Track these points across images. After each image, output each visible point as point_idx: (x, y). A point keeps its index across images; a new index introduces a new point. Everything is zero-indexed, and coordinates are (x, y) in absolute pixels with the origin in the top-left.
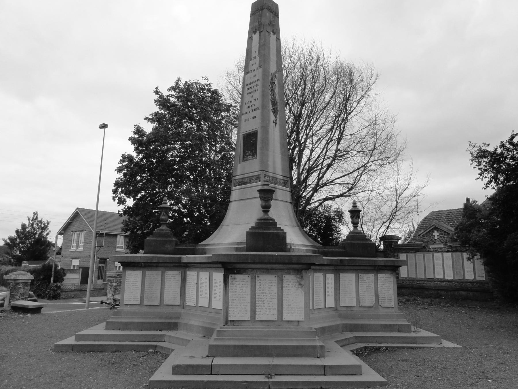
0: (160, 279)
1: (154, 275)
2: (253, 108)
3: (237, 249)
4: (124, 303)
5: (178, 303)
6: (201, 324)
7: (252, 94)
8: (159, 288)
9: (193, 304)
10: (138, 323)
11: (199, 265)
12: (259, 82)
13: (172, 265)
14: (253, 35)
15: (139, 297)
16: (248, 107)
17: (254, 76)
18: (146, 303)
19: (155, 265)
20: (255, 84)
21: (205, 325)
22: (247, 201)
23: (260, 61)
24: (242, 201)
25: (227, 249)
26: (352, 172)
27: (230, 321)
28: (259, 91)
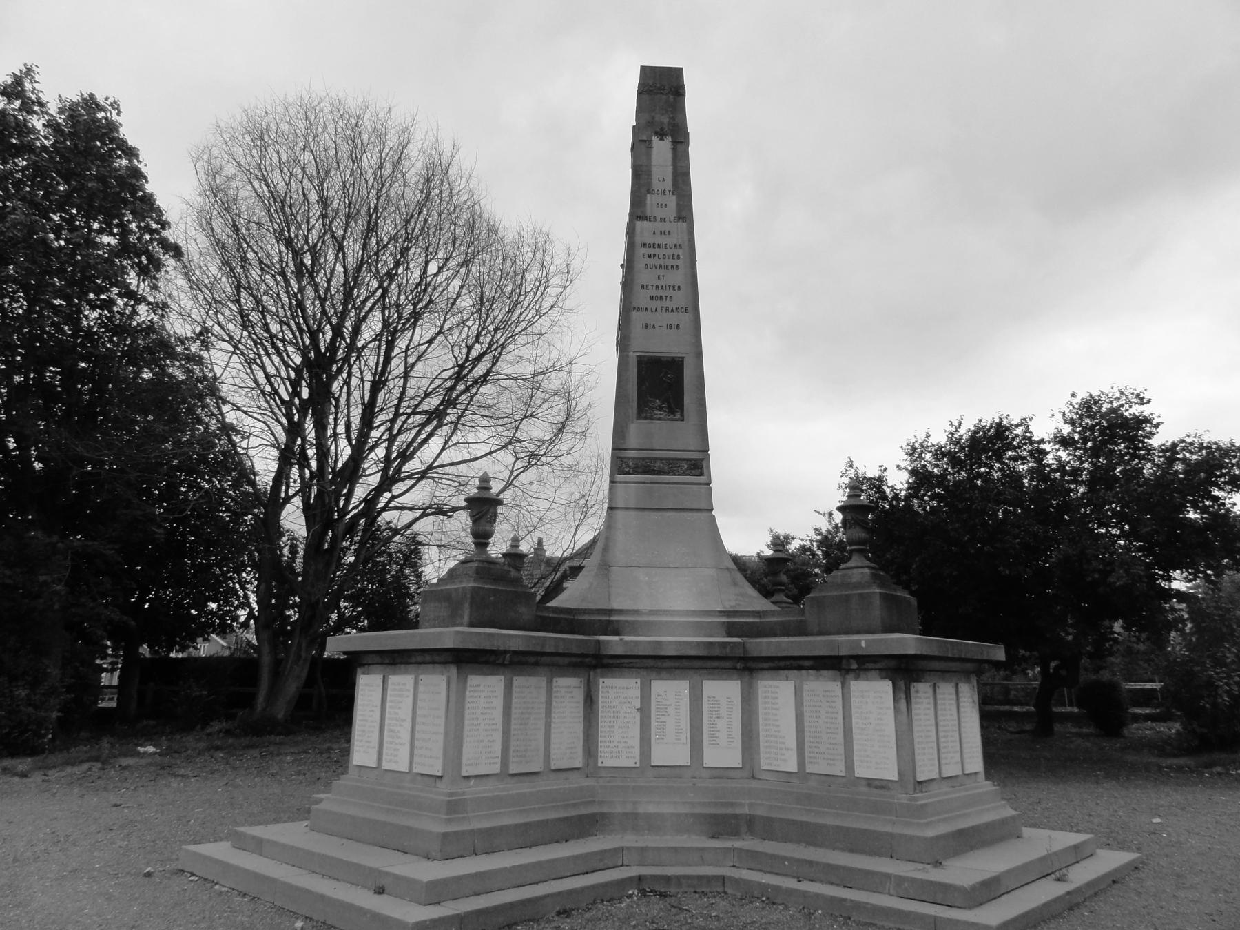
0: (543, 699)
1: (529, 687)
3: (731, 629)
4: (464, 773)
5: (578, 763)
6: (683, 810)
7: (661, 272)
9: (630, 759)
10: (516, 826)
11: (650, 662)
12: (680, 252)
13: (567, 660)
14: (655, 139)
15: (499, 753)
16: (651, 298)
18: (514, 769)
19: (532, 659)
20: (669, 252)
21: (698, 810)
23: (678, 205)
24: (646, 513)
25: (698, 627)
26: (477, 459)
28: (681, 271)
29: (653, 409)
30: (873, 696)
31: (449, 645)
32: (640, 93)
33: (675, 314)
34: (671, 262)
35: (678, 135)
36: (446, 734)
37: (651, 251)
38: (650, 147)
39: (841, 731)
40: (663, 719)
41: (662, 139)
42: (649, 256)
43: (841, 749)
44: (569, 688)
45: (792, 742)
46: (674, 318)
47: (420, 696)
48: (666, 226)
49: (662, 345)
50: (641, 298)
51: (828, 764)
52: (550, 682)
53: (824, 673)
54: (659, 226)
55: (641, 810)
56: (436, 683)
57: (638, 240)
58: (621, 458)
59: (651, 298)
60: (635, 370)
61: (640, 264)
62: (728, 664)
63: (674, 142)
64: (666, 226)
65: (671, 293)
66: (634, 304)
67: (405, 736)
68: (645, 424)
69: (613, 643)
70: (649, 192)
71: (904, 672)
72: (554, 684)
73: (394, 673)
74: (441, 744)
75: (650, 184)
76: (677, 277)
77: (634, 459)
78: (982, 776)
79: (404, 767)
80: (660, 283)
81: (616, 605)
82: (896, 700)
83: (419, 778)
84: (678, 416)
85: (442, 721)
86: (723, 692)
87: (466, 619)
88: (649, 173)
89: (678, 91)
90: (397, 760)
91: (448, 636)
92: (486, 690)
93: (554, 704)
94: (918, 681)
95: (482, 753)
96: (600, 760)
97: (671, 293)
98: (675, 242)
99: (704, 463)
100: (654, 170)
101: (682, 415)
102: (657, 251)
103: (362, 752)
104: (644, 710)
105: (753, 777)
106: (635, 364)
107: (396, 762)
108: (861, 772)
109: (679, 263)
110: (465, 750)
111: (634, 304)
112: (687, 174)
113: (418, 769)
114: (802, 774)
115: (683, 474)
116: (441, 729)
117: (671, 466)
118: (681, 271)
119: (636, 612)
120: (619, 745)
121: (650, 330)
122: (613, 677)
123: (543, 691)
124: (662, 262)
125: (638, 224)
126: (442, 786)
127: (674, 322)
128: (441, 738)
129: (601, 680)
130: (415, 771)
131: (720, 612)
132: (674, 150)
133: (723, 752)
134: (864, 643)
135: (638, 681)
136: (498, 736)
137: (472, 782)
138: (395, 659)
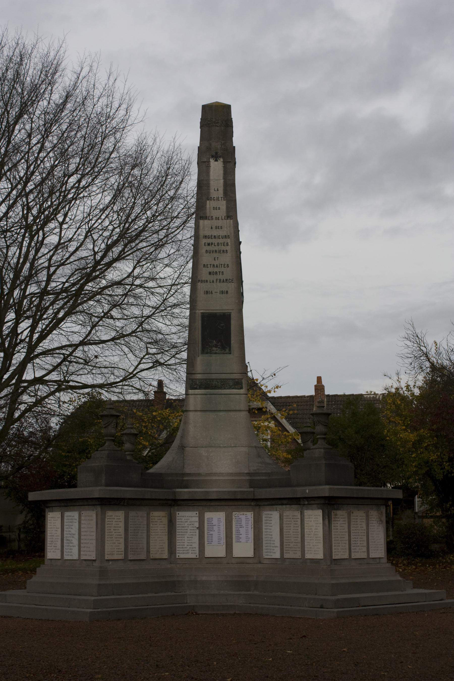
1: (138, 516)
2: (220, 277)
4: (106, 558)
5: (165, 556)
7: (216, 255)
8: (145, 535)
9: (193, 554)
12: (229, 241)
14: (212, 161)
15: (123, 549)
16: (210, 273)
17: (217, 228)
18: (131, 557)
20: (221, 241)
22: (221, 413)
23: (227, 208)
27: (334, 560)
28: (229, 254)
30: (314, 518)
31: (97, 496)
32: (201, 127)
33: (225, 284)
35: (228, 156)
36: (97, 540)
37: (210, 241)
38: (208, 166)
39: (300, 536)
40: (211, 533)
41: (216, 160)
42: (209, 244)
43: (299, 545)
44: (159, 517)
45: (278, 543)
46: (224, 287)
47: (82, 522)
48: (220, 223)
50: (204, 274)
51: (293, 554)
52: (148, 514)
53: (293, 506)
54: (215, 223)
55: (199, 579)
56: (90, 516)
57: (202, 233)
58: (192, 380)
59: (210, 273)
60: (200, 322)
61: (203, 249)
62: (247, 503)
63: (225, 162)
64: (220, 223)
65: (222, 269)
67: (76, 542)
69: (184, 493)
70: (208, 200)
71: (329, 504)
72: (151, 515)
73: (67, 511)
74: (95, 544)
75: (209, 193)
77: (199, 379)
78: (385, 560)
79: (76, 557)
80: (216, 263)
81: (187, 471)
82: (323, 520)
83: (84, 562)
84: (227, 351)
85: (94, 534)
86: (244, 519)
87: (103, 481)
88: (208, 185)
89: (228, 124)
90: (72, 554)
91: (97, 492)
92: (116, 518)
93: (151, 525)
94: (338, 509)
95: (114, 548)
96: (177, 555)
97: (222, 269)
98: (225, 233)
100: (211, 182)
102: (213, 241)
103: (52, 552)
104: (201, 528)
105: (260, 563)
106: (200, 318)
107: (72, 555)
108: (308, 556)
109: (228, 248)
110: (106, 547)
112: (234, 185)
113: (83, 558)
114: (282, 558)
115: (230, 388)
116: (94, 537)
118: (229, 254)
119: (199, 475)
120: (187, 547)
122: (185, 511)
123: (145, 518)
124: (216, 248)
125: (201, 222)
126: (96, 564)
127: (224, 289)
128: (94, 542)
129: (177, 513)
130: (82, 558)
131: (247, 473)
132: (225, 169)
133: (244, 549)
134: (308, 491)
135: (198, 513)
136: (122, 541)
137: (111, 563)
138: (67, 504)
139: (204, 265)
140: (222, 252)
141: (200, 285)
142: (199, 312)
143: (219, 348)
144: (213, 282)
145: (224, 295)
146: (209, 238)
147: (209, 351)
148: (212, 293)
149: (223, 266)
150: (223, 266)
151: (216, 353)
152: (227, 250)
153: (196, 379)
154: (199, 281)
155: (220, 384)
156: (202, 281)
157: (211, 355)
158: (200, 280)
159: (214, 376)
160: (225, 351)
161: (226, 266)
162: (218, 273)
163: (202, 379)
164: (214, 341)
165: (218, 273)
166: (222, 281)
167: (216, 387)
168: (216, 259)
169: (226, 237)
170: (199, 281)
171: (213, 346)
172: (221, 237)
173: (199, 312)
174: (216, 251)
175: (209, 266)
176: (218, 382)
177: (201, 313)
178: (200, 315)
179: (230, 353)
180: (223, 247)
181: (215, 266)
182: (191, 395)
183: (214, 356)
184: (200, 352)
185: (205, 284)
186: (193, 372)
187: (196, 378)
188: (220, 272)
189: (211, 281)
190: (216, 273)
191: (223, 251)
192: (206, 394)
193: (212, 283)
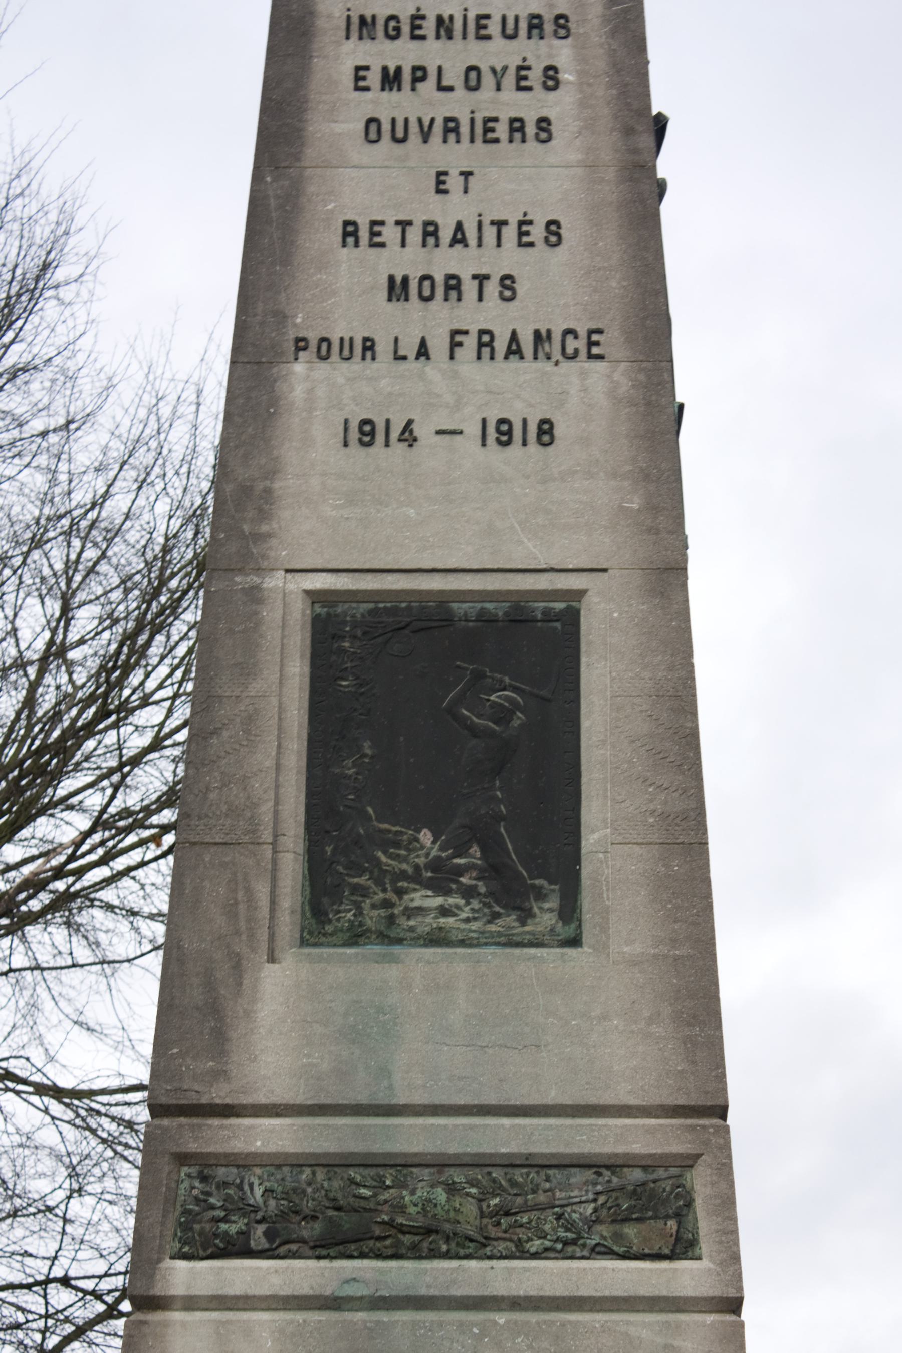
7: (454, 156)
12: (562, 53)
20: (497, 53)
28: (566, 147)
29: (400, 883)
33: (526, 370)
34: (510, 103)
37: (403, 53)
42: (391, 79)
49: (451, 524)
50: (343, 291)
58: (204, 1166)
59: (397, 289)
61: (337, 117)
65: (508, 258)
66: (303, 322)
68: (347, 970)
76: (550, 180)
77: (277, 1162)
80: (449, 212)
84: (545, 918)
99: (700, 1181)
101: (570, 910)
102: (431, 52)
109: (559, 107)
111: (303, 322)
115: (569, 1246)
117: (505, 1206)
118: (566, 147)
121: (389, 457)
124: (459, 105)
127: (523, 409)
139: (350, 231)
140: (502, 130)
141: (301, 377)
142: (285, 599)
143: (469, 893)
144: (423, 351)
145: (515, 449)
146: (394, 35)
147: (373, 917)
148: (408, 436)
149: (510, 233)
150: (510, 233)
151: (437, 939)
152: (544, 124)
153: (244, 1162)
154: (301, 344)
155: (470, 1209)
156: (324, 349)
157: (397, 949)
158: (313, 337)
159: (413, 1137)
160: (526, 915)
161: (537, 232)
162: (469, 288)
163: (297, 1163)
164: (426, 837)
165: (469, 288)
166: (501, 346)
167: (430, 1238)
168: (454, 182)
169: (535, 24)
170: (301, 344)
171: (416, 878)
172: (494, 27)
173: (285, 599)
174: (451, 127)
175: (390, 234)
176: (452, 1189)
177: (315, 597)
178: (299, 614)
179: (575, 942)
180: (509, 94)
181: (446, 234)
182: (191, 1303)
183: (418, 963)
184: (288, 922)
185: (356, 366)
186: (219, 1095)
187: (238, 1145)
188: (481, 279)
189: (409, 348)
190: (453, 284)
191: (517, 126)
192: (333, 1303)
193: (412, 365)
